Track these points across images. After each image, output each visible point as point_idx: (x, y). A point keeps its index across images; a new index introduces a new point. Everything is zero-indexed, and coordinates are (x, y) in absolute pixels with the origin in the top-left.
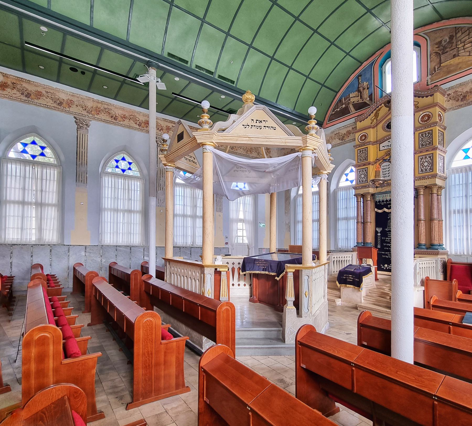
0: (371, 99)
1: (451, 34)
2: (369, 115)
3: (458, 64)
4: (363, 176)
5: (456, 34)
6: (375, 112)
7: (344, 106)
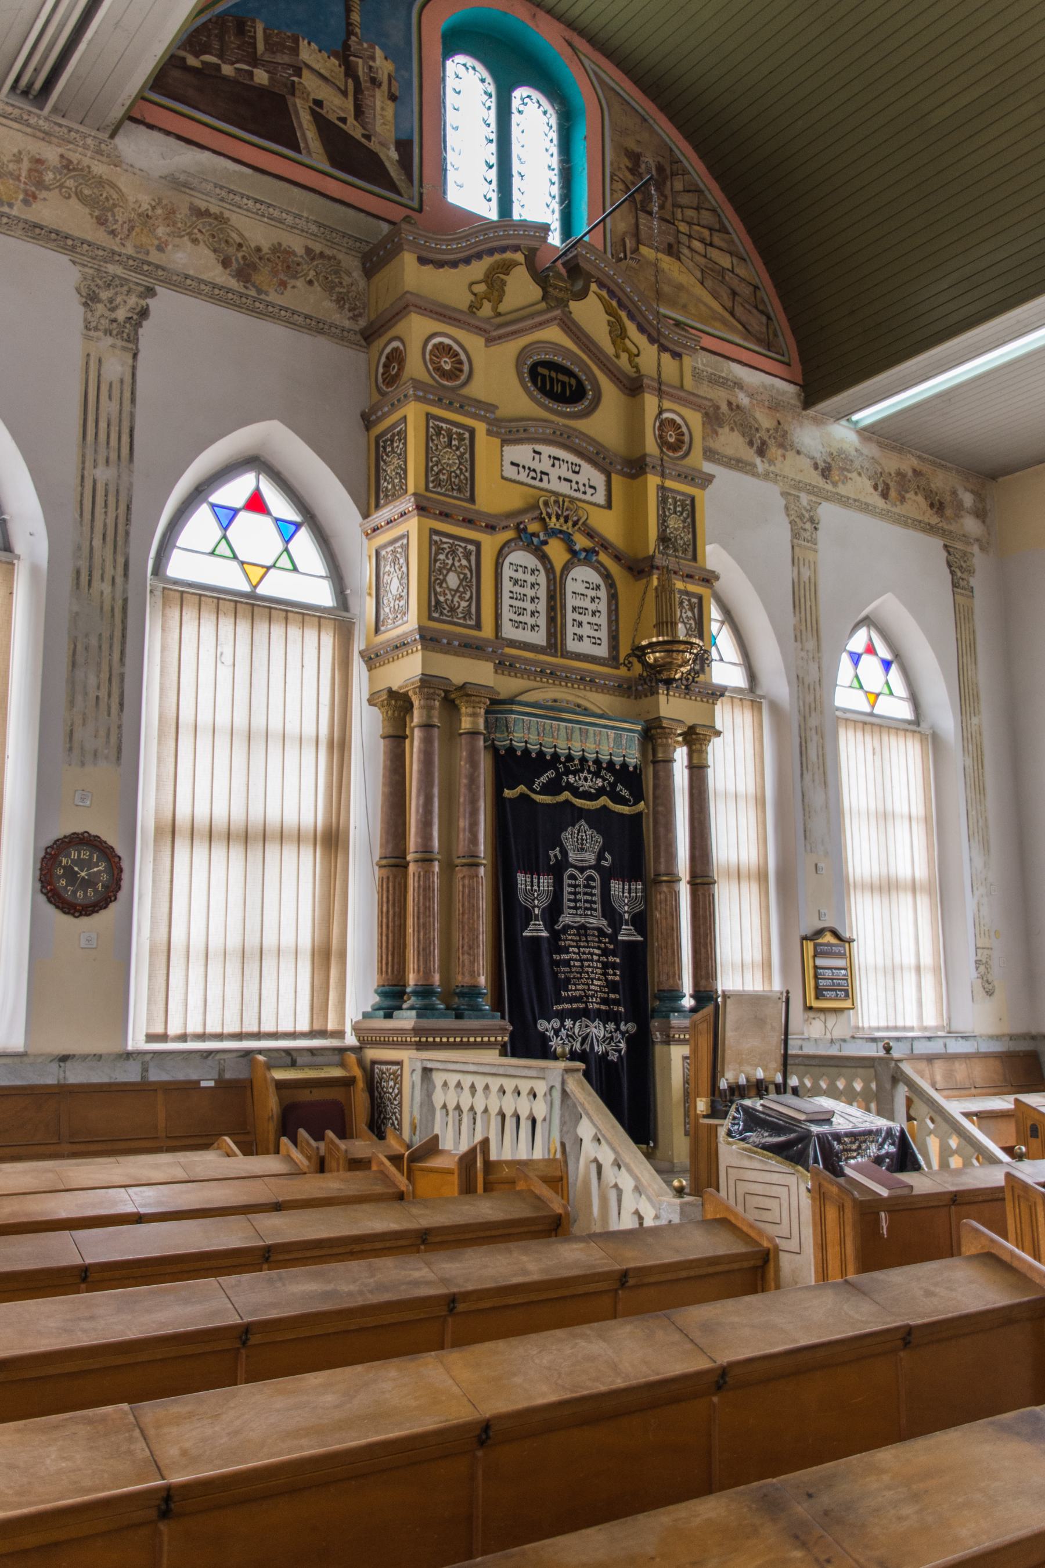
0: (405, 163)
1: (660, 159)
2: (467, 261)
3: (680, 287)
4: (453, 581)
5: (672, 175)
6: (488, 261)
7: (261, 77)
